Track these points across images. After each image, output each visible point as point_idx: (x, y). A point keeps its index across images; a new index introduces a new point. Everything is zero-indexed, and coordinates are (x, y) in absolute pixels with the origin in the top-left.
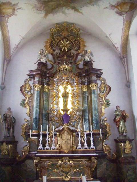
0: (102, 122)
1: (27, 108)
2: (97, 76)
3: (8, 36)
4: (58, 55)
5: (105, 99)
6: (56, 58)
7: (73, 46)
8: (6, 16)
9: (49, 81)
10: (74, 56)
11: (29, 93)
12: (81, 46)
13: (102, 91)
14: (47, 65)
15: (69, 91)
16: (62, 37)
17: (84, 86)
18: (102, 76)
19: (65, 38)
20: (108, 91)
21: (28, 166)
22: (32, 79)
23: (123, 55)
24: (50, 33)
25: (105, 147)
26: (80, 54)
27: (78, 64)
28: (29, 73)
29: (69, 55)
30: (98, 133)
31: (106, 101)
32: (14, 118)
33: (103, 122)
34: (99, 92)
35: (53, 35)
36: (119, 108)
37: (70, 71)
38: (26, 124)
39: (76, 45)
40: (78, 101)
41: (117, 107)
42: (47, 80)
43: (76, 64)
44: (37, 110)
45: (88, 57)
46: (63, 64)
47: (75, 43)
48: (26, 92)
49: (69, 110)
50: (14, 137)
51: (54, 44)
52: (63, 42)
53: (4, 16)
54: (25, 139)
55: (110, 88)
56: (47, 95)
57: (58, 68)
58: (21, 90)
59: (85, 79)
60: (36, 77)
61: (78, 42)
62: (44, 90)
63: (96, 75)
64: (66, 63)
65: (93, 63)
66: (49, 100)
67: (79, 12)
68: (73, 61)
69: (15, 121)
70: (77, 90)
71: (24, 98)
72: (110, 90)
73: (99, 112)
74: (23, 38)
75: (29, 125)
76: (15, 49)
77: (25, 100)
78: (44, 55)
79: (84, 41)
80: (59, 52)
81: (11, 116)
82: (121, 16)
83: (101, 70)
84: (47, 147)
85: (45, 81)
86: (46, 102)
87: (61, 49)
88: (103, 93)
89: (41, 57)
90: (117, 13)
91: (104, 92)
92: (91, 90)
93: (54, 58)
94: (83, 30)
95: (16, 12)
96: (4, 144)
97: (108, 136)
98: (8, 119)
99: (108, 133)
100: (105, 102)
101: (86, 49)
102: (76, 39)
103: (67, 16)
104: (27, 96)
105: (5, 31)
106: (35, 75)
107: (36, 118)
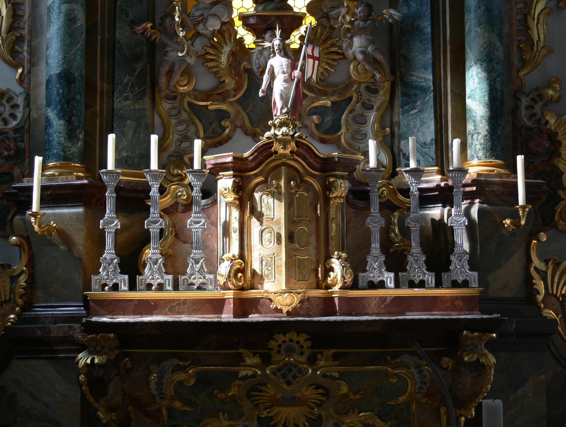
25: (545, 280)
30: (503, 184)
33: (537, 109)
44: (70, 20)
49: (298, 20)
75: (14, 123)
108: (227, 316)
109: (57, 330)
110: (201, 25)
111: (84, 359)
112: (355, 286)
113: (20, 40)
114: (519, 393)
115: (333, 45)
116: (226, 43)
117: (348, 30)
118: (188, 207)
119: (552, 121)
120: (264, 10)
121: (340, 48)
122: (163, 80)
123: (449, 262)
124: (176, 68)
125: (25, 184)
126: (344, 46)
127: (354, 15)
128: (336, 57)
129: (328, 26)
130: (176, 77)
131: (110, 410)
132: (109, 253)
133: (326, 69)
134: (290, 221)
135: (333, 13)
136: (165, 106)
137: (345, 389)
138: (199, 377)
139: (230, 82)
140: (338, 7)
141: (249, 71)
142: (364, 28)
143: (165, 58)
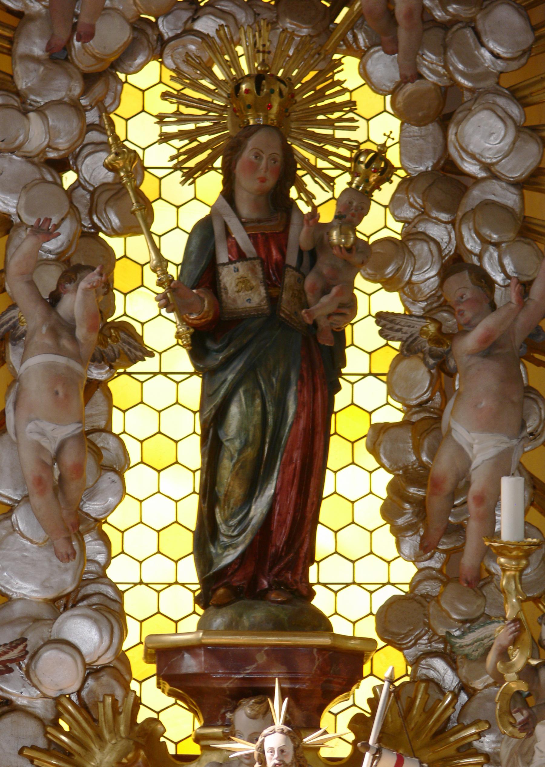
116: (100, 736)
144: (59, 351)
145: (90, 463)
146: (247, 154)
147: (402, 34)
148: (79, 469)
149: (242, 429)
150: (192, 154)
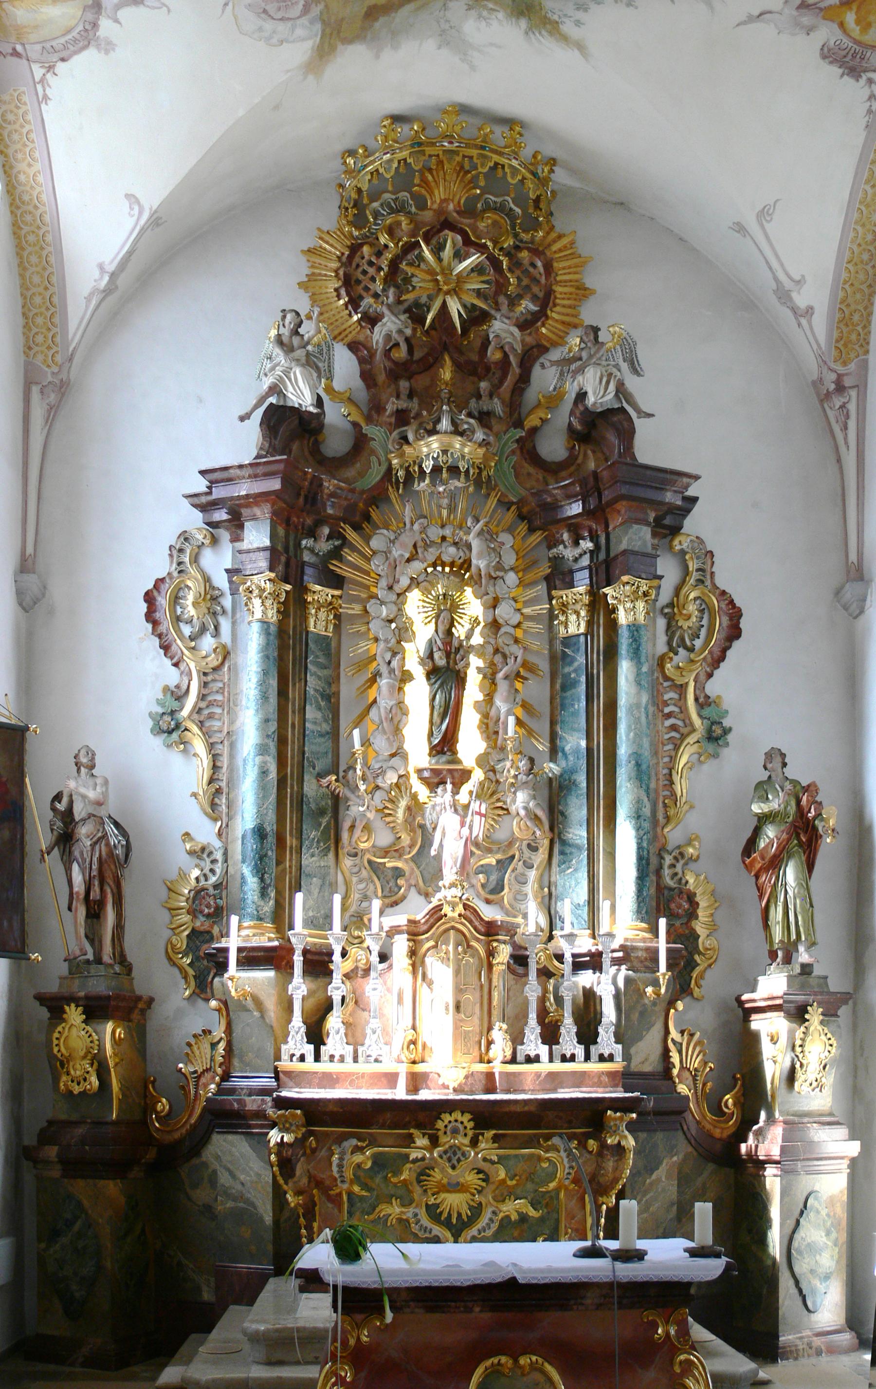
0: (673, 866)
1: (195, 755)
2: (658, 522)
3: (44, 197)
4: (401, 354)
5: (696, 699)
6: (381, 378)
7: (500, 287)
8: (38, 47)
9: (336, 554)
10: (505, 363)
11: (208, 643)
12: (558, 289)
13: (682, 639)
14: (322, 426)
15: (469, 637)
16: (427, 216)
17: (567, 595)
18: (690, 524)
19: (448, 225)
20: (723, 635)
21: (224, 1179)
22: (224, 535)
23: (841, 369)
24: (341, 186)
25: (680, 1052)
26: (546, 350)
27: (534, 431)
28: (200, 485)
29: (475, 357)
30: (647, 949)
31: (706, 712)
32: (117, 824)
33: (679, 868)
34: (661, 647)
35: (365, 201)
36: (784, 765)
37: (478, 483)
38: (196, 873)
39: (518, 278)
40: (525, 705)
41: (769, 756)
42: (324, 546)
43: (519, 424)
45: (610, 375)
46: (430, 427)
47: (515, 264)
48: (187, 630)
50: (121, 958)
51: (371, 271)
52: (437, 251)
53: (19, 48)
54: (193, 983)
55: (735, 615)
56: (327, 652)
57: (402, 455)
58: (150, 616)
59: (576, 543)
60: (254, 518)
61: (539, 264)
62: (305, 618)
63: (652, 516)
64: (454, 423)
65: (638, 423)
66: (337, 694)
67: (565, 39)
68: (497, 406)
69: (128, 848)
70: (518, 626)
71: (172, 677)
72: (734, 633)
73: (656, 791)
74: (156, 221)
75: (213, 879)
76: (94, 303)
77: (179, 695)
78: (300, 353)
79: (583, 249)
80: (408, 332)
81: (103, 812)
82: (857, 78)
83: (685, 480)
84: (334, 1044)
85: (311, 550)
86: (319, 715)
87: (416, 314)
88: (691, 650)
89: (287, 372)
90: (828, 54)
91: (698, 643)
92: (612, 625)
93: (367, 376)
94: (573, 171)
95: (106, 26)
96: (74, 1015)
97: (701, 976)
98: (84, 831)
99: (700, 953)
100: (697, 721)
101: (589, 314)
102: (525, 237)
103: (473, 68)
104: (192, 665)
105: (30, 165)
106: (248, 506)
107: (260, 832)
108: (400, 1093)
109: (252, 1103)
110: (380, 777)
111: (274, 1136)
112: (513, 1060)
113: (218, 791)
114: (654, 1177)
115: (498, 800)
116: (402, 797)
117: (512, 784)
118: (367, 971)
119: (691, 881)
120: (437, 763)
121: (505, 803)
122: (345, 835)
123: (597, 1034)
124: (357, 824)
125: (223, 945)
126: (508, 801)
127: (518, 768)
128: (501, 812)
129: (494, 780)
130: (357, 832)
131: (298, 1193)
132: (297, 1023)
133: (492, 825)
134: (459, 990)
135: (499, 766)
136: (347, 862)
137: (502, 1174)
138: (376, 1158)
139: (406, 839)
140: (504, 759)
141: (422, 827)
142: (526, 783)
143: (348, 812)
144: (391, 678)
145: (399, 712)
146: (441, 618)
147: (483, 581)
148: (396, 714)
149: (440, 702)
150: (426, 618)
